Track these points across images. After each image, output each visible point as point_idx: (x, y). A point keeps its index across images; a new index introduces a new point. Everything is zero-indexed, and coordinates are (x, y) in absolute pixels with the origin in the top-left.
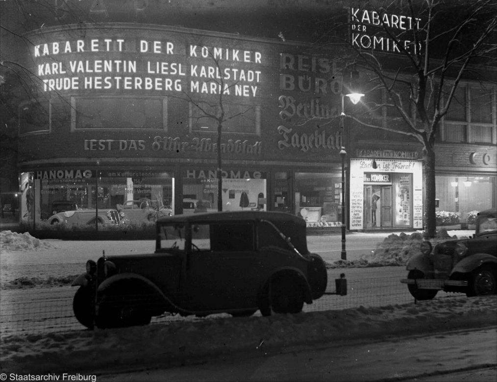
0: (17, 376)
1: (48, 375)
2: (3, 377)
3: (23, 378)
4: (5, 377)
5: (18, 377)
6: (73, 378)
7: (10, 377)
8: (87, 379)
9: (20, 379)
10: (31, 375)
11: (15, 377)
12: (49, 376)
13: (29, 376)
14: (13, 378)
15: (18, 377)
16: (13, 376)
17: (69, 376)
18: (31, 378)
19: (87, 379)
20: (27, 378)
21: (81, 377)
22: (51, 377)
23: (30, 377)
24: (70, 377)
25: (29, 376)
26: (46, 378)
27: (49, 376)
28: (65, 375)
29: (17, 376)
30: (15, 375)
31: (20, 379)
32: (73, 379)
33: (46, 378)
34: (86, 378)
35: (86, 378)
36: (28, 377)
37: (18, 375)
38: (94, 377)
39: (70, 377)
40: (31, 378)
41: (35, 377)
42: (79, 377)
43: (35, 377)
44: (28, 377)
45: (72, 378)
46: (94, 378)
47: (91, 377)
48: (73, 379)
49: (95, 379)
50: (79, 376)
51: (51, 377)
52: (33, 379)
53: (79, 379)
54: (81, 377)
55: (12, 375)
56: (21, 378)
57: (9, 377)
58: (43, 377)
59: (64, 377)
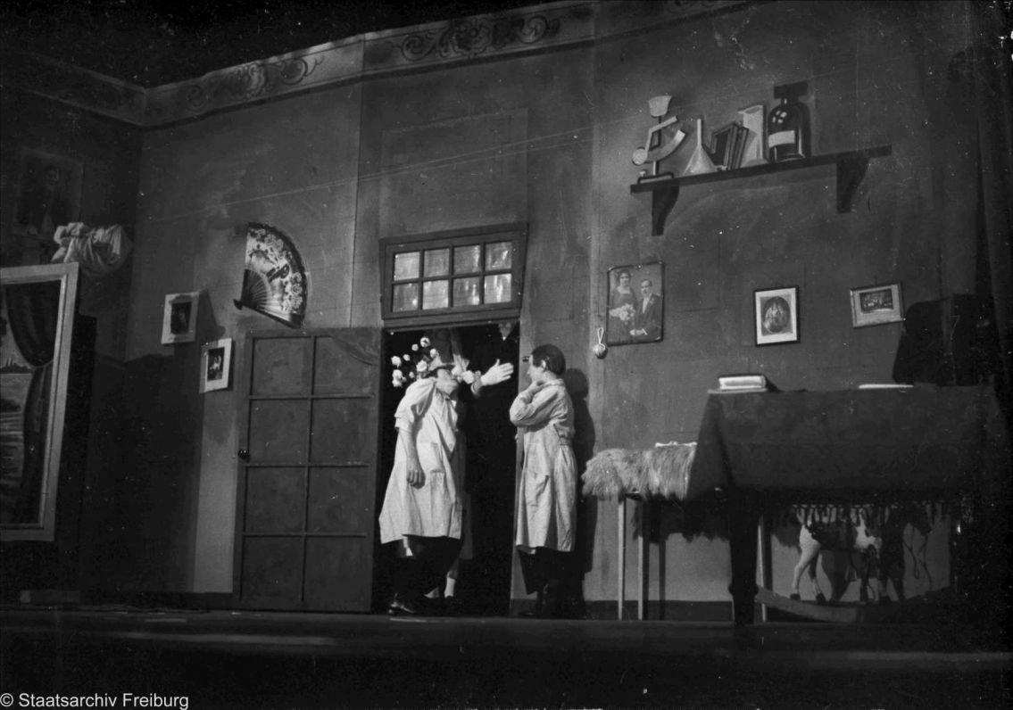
0: (33, 698)
2: (7, 700)
3: (46, 701)
4: (11, 700)
5: (35, 701)
6: (143, 701)
7: (22, 701)
8: (171, 705)
9: (40, 704)
10: (61, 696)
13: (57, 697)
14: (25, 703)
16: (26, 699)
17: (135, 699)
18: (60, 702)
19: (171, 705)
20: (53, 701)
21: (158, 702)
22: (99, 700)
23: (60, 700)
24: (138, 701)
25: (57, 697)
26: (90, 702)
27: (96, 699)
28: (127, 697)
29: (33, 698)
31: (40, 704)
33: (90, 702)
34: (168, 703)
35: (168, 703)
36: (55, 700)
37: (36, 696)
38: (184, 702)
39: (138, 701)
40: (60, 702)
41: (69, 701)
42: (155, 700)
43: (69, 701)
44: (55, 700)
45: (141, 701)
46: (184, 702)
47: (178, 700)
49: (187, 705)
50: (155, 699)
51: (99, 700)
52: (65, 704)
54: (158, 702)
55: (24, 697)
56: (42, 702)
57: (17, 700)
58: (84, 701)
59: (125, 700)
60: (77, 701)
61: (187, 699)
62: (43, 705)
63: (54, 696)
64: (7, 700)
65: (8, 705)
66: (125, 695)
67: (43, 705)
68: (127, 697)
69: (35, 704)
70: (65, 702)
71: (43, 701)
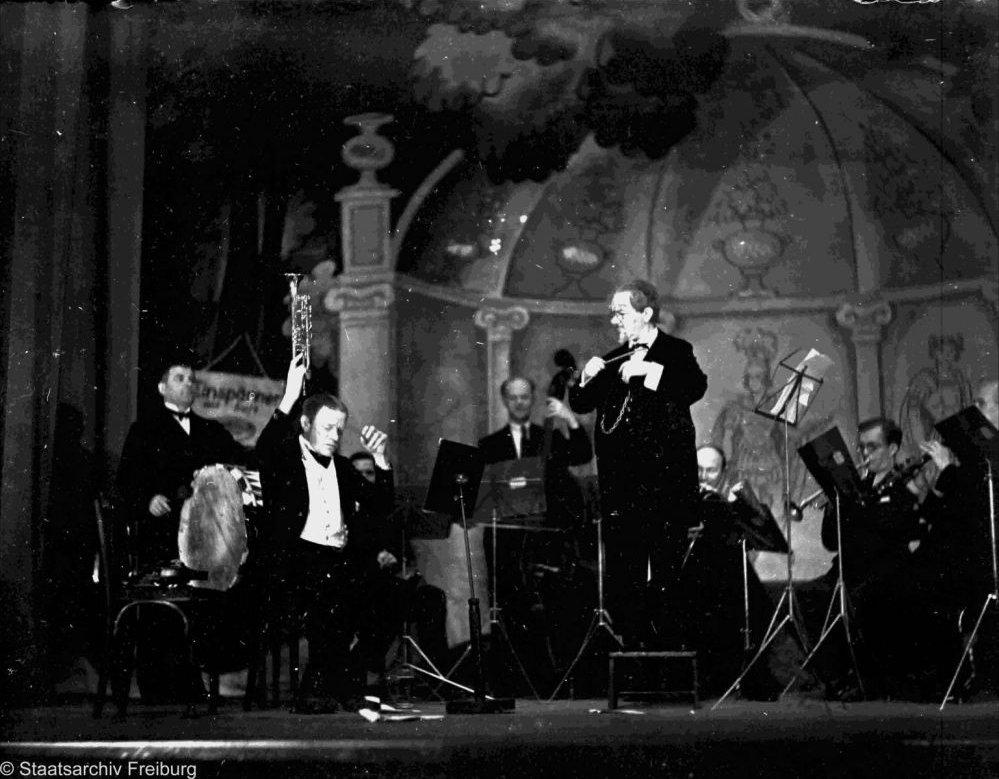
0: (34, 766)
1: (98, 765)
2: (7, 769)
3: (47, 770)
5: (37, 770)
10: (63, 765)
11: (32, 769)
12: (101, 767)
13: (60, 766)
14: (26, 772)
15: (37, 770)
16: (27, 768)
17: (141, 767)
18: (63, 771)
21: (165, 770)
22: (103, 769)
23: (62, 769)
24: (144, 769)
25: (60, 766)
26: (94, 770)
27: (101, 767)
28: (132, 765)
29: (34, 766)
30: (32, 764)
31: (41, 773)
32: (150, 772)
33: (94, 770)
34: (175, 771)
35: (175, 771)
36: (58, 769)
37: (37, 765)
38: (192, 770)
39: (144, 769)
40: (63, 771)
44: (58, 769)
45: (147, 770)
46: (192, 770)
48: (150, 772)
49: (195, 773)
51: (103, 769)
52: (67, 772)
53: (162, 774)
54: (165, 770)
55: (25, 765)
56: (43, 770)
57: (18, 769)
58: (88, 769)
59: (130, 768)
60: (80, 770)
61: (195, 767)
62: (45, 774)
63: (57, 765)
64: (7, 769)
65: (9, 773)
66: (130, 763)
67: (45, 774)
68: (132, 765)
69: (36, 772)
70: (68, 770)
71: (45, 770)
